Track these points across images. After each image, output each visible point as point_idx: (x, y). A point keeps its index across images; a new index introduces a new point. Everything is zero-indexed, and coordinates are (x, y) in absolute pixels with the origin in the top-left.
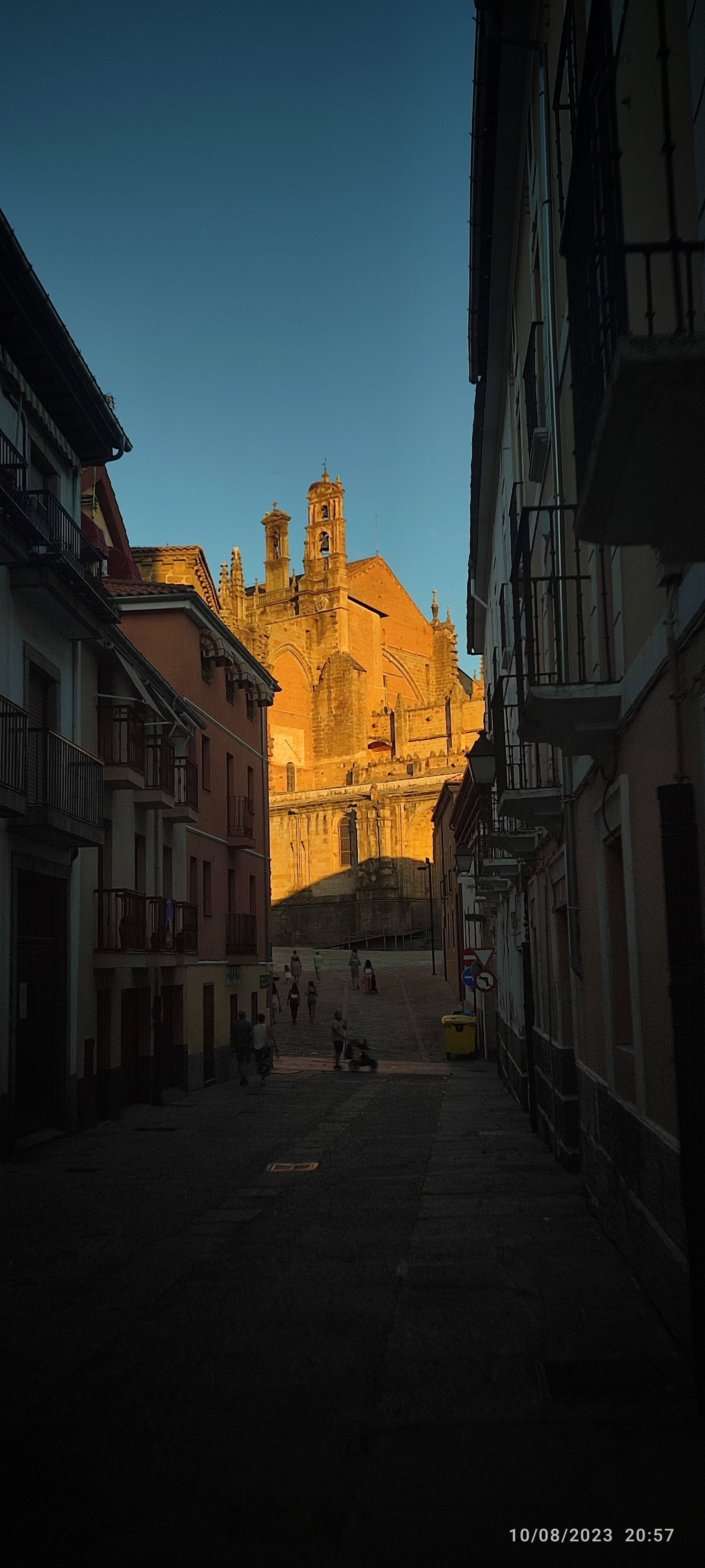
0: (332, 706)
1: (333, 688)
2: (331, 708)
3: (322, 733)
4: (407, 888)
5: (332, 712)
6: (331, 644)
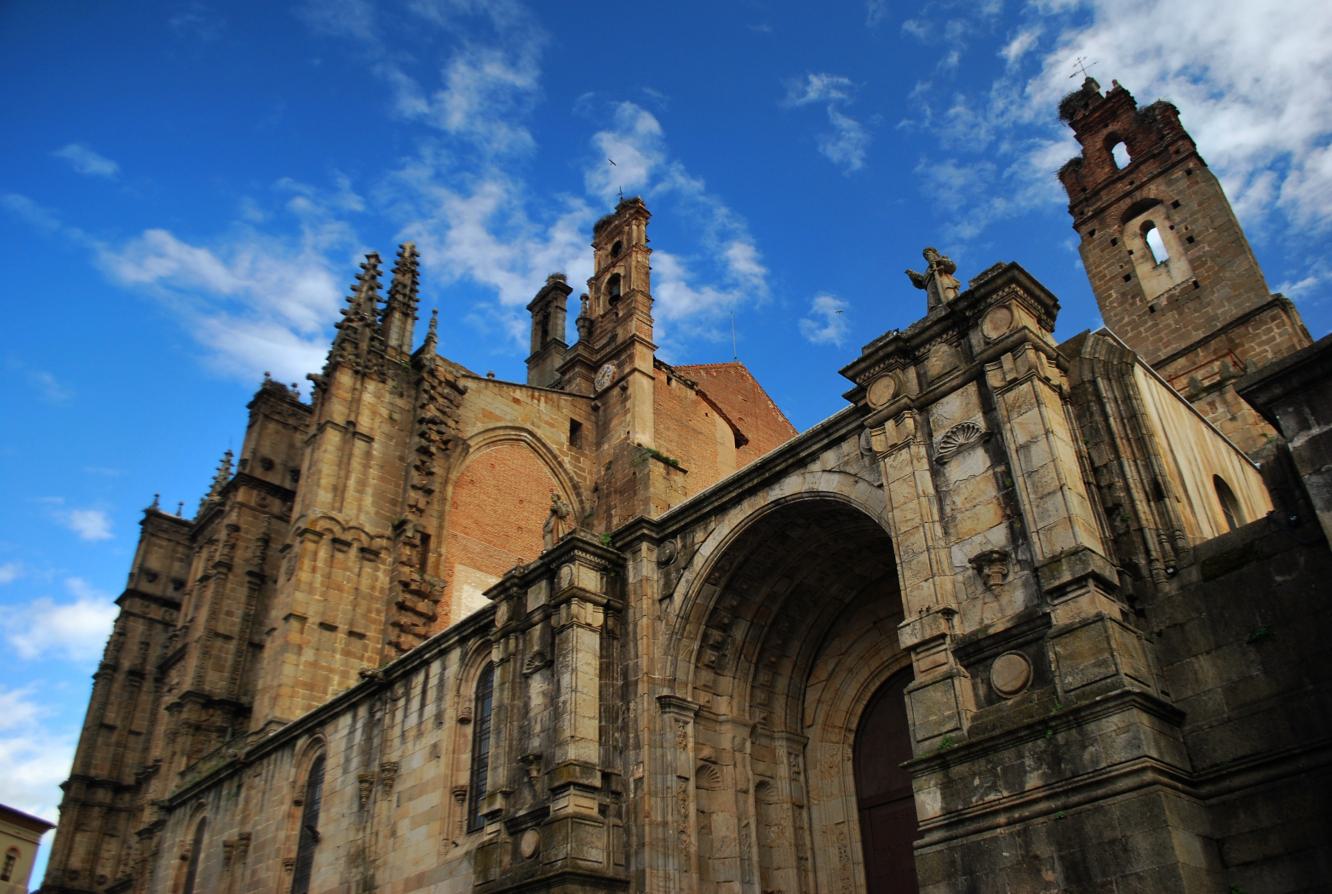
4: (667, 878)
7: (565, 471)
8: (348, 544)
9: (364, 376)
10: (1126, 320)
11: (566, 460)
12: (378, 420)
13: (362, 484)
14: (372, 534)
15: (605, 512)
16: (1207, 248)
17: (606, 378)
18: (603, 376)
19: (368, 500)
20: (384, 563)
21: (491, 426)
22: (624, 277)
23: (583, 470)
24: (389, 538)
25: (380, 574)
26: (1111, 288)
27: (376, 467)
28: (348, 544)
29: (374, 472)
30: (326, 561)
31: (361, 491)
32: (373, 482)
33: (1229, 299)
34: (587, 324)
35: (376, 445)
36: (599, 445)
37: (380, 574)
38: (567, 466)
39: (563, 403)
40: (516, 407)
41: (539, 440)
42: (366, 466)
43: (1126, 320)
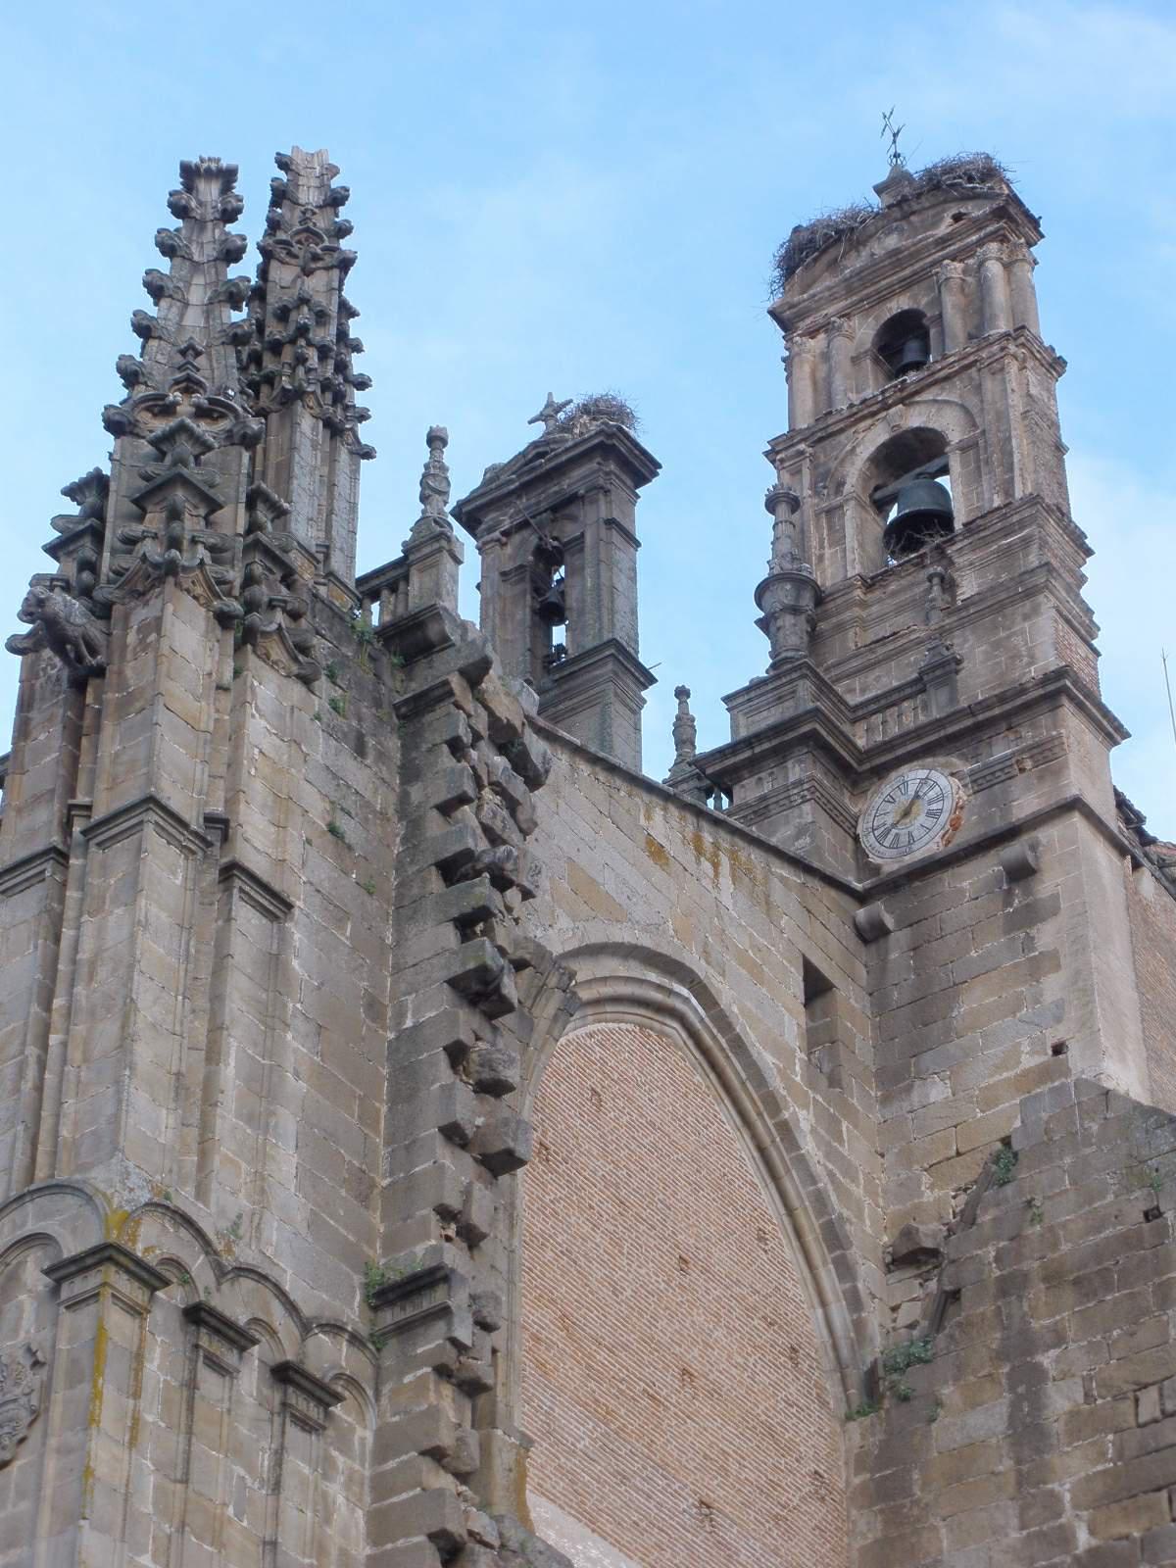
0: (1064, 1489)
2: (1053, 1504)
5: (1065, 1538)
6: (1013, 1055)
7: (802, 1161)
8: (239, 1338)
9: (248, 637)
11: (804, 1120)
12: (296, 834)
13: (264, 1085)
14: (307, 1310)
15: (1001, 1356)
17: (922, 819)
18: (906, 813)
19: (286, 1162)
20: (344, 1444)
21: (597, 935)
22: (965, 448)
23: (849, 1171)
24: (355, 1339)
25: (336, 1491)
27: (299, 1023)
28: (239, 1338)
29: (295, 1044)
30: (166, 1403)
31: (259, 1120)
32: (297, 1087)
34: (807, 601)
35: (298, 933)
36: (895, 1080)
37: (336, 1491)
38: (809, 1146)
39: (778, 893)
40: (658, 874)
41: (723, 1022)
42: (272, 1018)
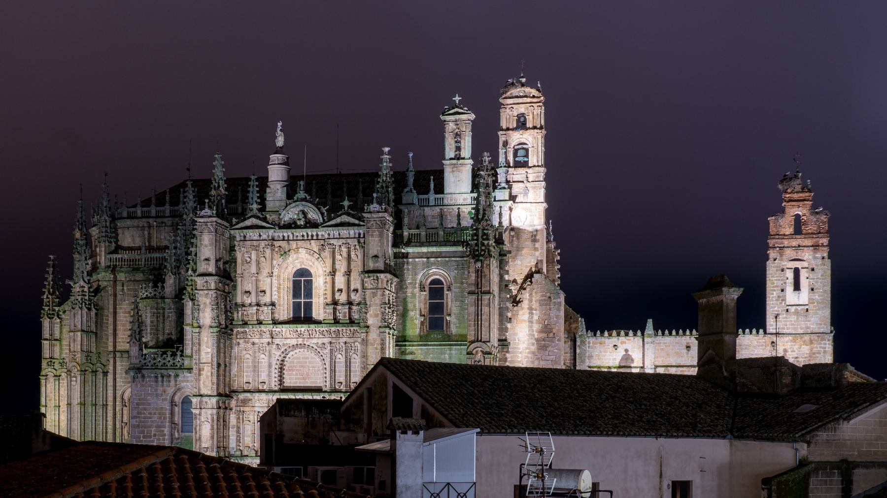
1: (536, 310)
3: (520, 355)
10: (776, 309)
16: (817, 297)
26: (775, 290)
33: (817, 324)
43: (776, 309)
